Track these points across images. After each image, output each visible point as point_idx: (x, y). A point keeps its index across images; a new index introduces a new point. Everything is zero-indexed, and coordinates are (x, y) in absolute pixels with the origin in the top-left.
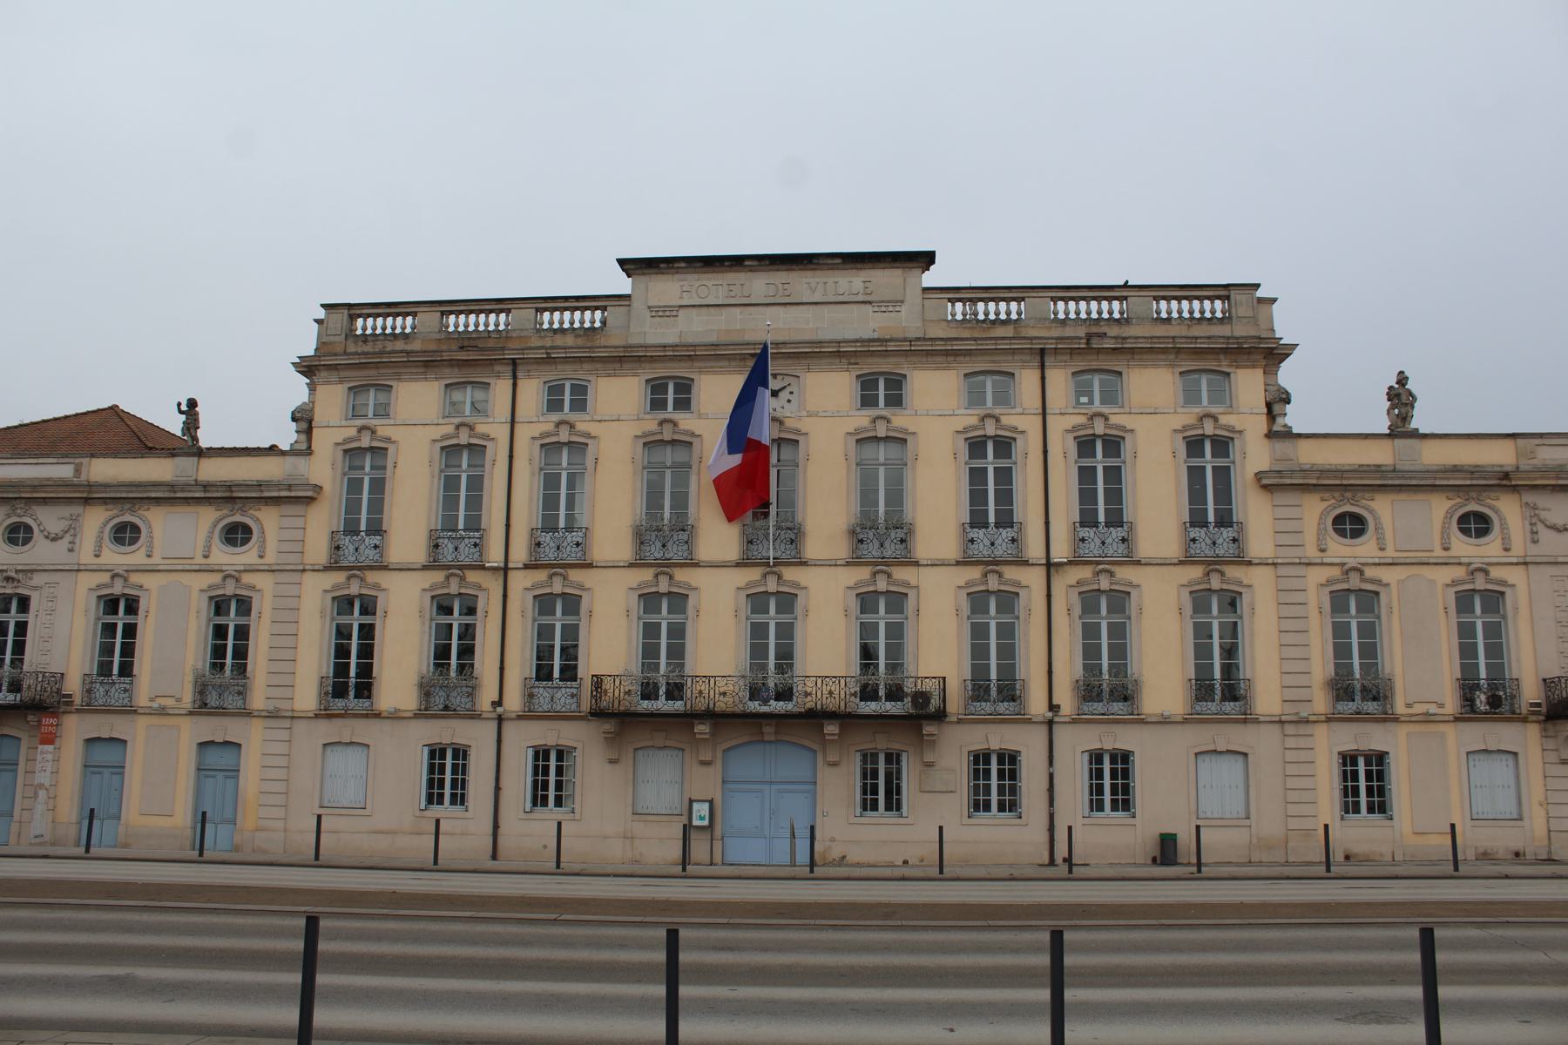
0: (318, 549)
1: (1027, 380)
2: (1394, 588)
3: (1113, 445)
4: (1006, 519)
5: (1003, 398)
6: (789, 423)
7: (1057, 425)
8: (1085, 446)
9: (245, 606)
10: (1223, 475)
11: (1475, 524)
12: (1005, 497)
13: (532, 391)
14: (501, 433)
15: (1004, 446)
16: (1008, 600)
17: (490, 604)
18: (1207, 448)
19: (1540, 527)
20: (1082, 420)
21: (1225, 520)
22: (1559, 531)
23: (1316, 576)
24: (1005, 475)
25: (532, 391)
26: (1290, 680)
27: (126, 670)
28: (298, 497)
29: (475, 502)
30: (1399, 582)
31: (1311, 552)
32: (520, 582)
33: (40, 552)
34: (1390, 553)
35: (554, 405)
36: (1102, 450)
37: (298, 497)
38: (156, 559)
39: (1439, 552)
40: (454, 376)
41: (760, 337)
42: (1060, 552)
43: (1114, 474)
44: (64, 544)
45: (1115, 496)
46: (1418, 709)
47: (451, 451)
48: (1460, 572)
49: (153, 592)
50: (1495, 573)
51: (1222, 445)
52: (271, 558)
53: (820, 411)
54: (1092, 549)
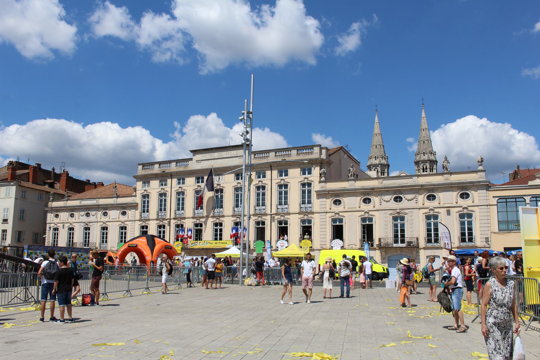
0: (138, 217)
1: (268, 173)
2: (347, 217)
3: (286, 186)
4: (263, 205)
5: (264, 176)
6: (222, 185)
7: (274, 182)
8: (280, 186)
9: (126, 228)
10: (309, 192)
11: (367, 201)
12: (263, 199)
13: (175, 181)
14: (169, 190)
15: (264, 188)
16: (263, 223)
17: (167, 227)
18: (306, 185)
19: (382, 201)
20: (280, 181)
21: (310, 202)
22: (387, 202)
23: (329, 215)
24: (264, 194)
25: (175, 181)
26: (322, 240)
27: (106, 242)
28: (134, 206)
29: (165, 205)
30: (348, 216)
31: (328, 210)
32: (173, 222)
33: (91, 218)
34: (346, 209)
35: (179, 183)
36: (283, 186)
37: (134, 206)
38: (111, 220)
39: (358, 209)
40: (161, 179)
41: (211, 167)
42: (274, 211)
43: (286, 193)
44: (95, 217)
45: (286, 198)
46: (351, 246)
47: (161, 195)
48: (363, 213)
49: (110, 226)
50: (371, 213)
51: (309, 185)
52: (130, 219)
53: (227, 182)
54: (280, 211)
